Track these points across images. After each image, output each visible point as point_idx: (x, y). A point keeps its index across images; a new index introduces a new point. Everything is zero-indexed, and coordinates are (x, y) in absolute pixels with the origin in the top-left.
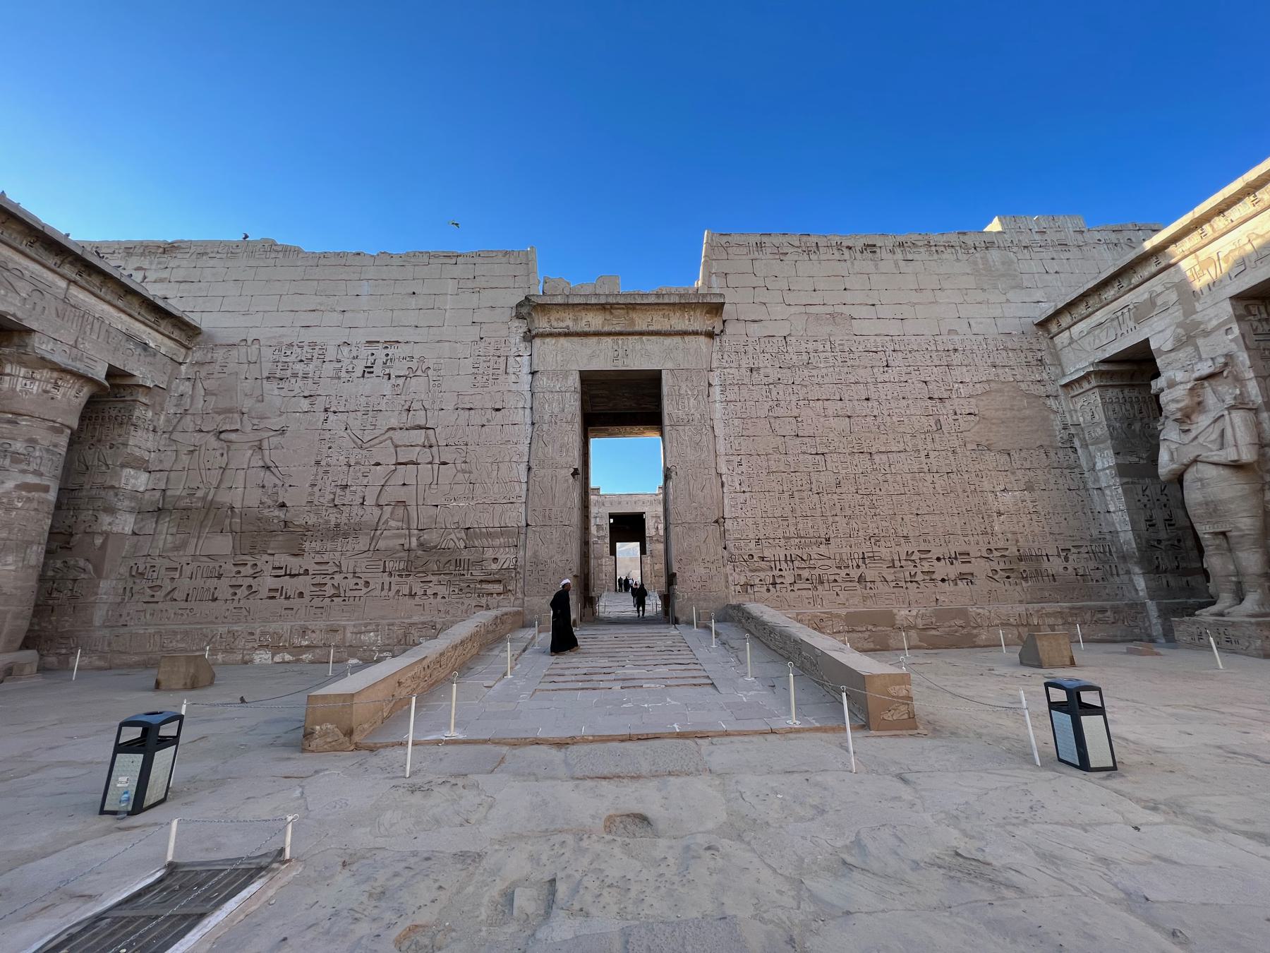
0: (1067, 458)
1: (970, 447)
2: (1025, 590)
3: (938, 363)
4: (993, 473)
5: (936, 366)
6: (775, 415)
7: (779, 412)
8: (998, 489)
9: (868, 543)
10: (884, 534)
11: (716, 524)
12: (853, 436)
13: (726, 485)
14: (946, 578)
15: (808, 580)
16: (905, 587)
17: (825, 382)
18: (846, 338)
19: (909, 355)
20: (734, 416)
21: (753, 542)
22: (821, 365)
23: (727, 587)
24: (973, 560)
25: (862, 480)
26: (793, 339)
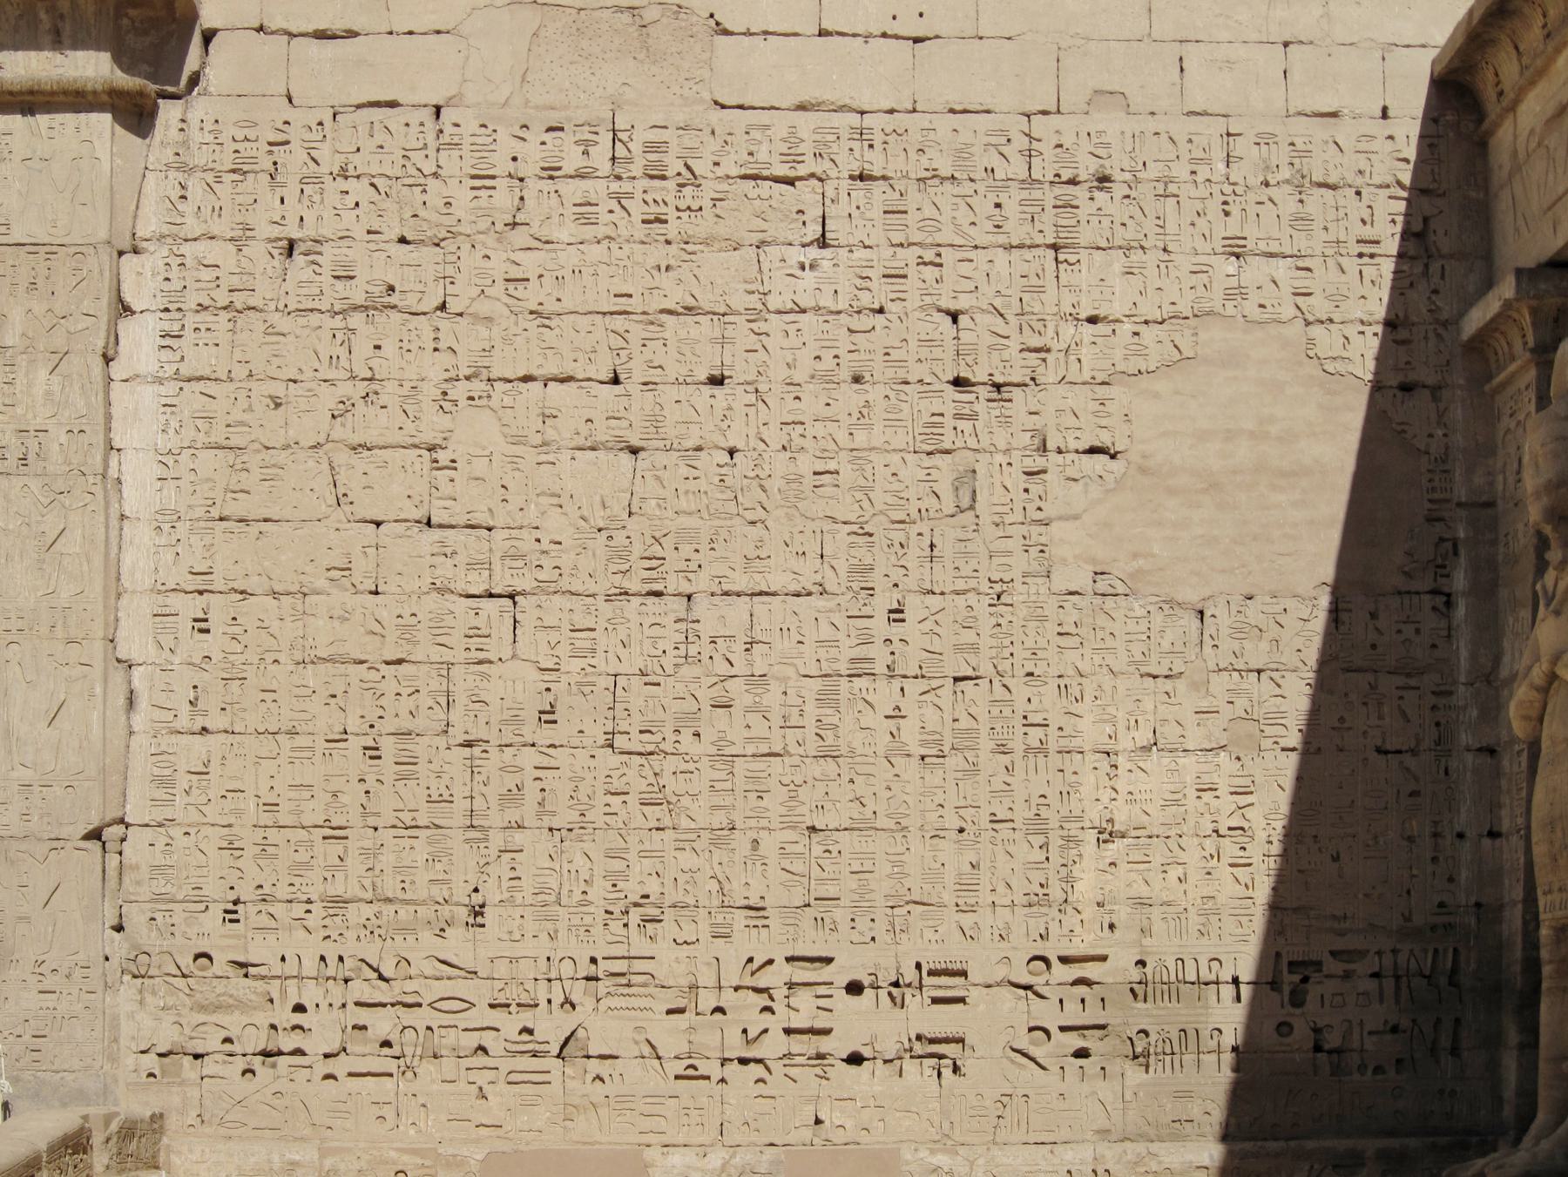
0: (1409, 630)
1: (1060, 582)
2: (1128, 1097)
3: (1017, 231)
4: (1122, 684)
5: (1009, 247)
6: (356, 439)
7: (373, 424)
8: (1125, 743)
9: (616, 926)
10: (680, 897)
11: (94, 846)
12: (633, 525)
13: (143, 703)
14: (866, 1052)
15: (386, 1044)
16: (716, 1073)
17: (567, 304)
18: (680, 117)
19: (914, 198)
20: (202, 439)
21: (217, 911)
22: (563, 235)
23: (113, 1059)
24: (974, 994)
25: (636, 695)
26: (469, 126)
